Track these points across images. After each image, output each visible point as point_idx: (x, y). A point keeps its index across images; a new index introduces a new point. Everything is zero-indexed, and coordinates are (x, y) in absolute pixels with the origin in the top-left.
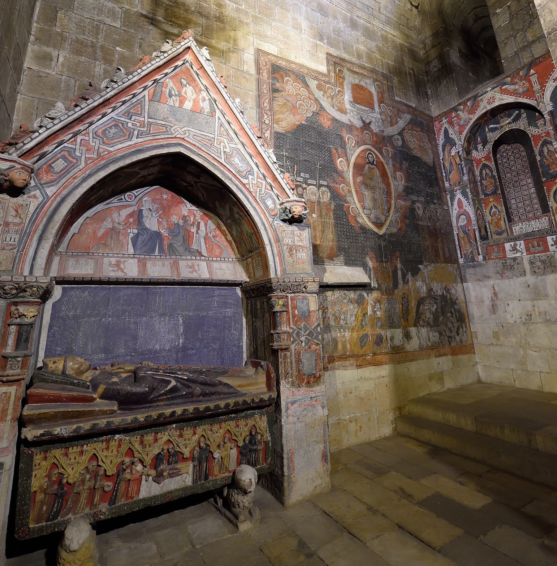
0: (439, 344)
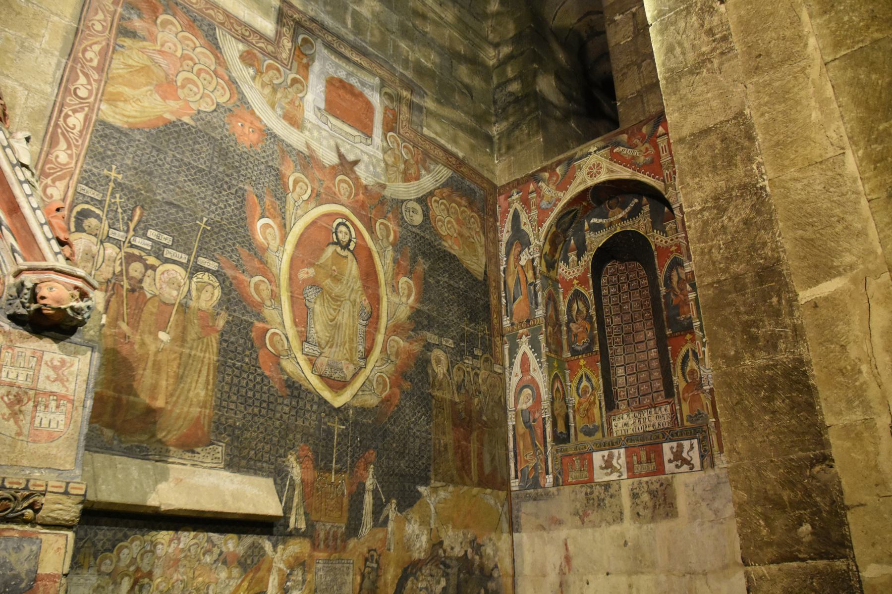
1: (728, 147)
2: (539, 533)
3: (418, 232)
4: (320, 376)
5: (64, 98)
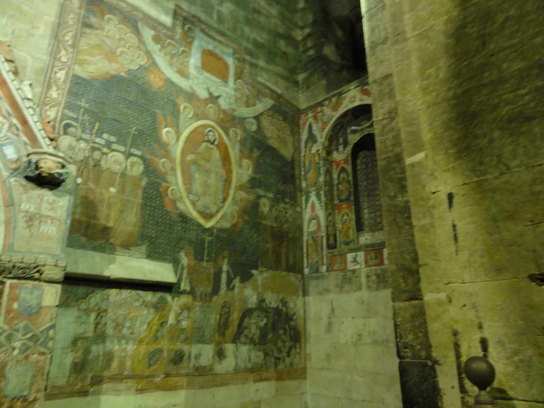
3: (254, 135)
5: (53, 63)
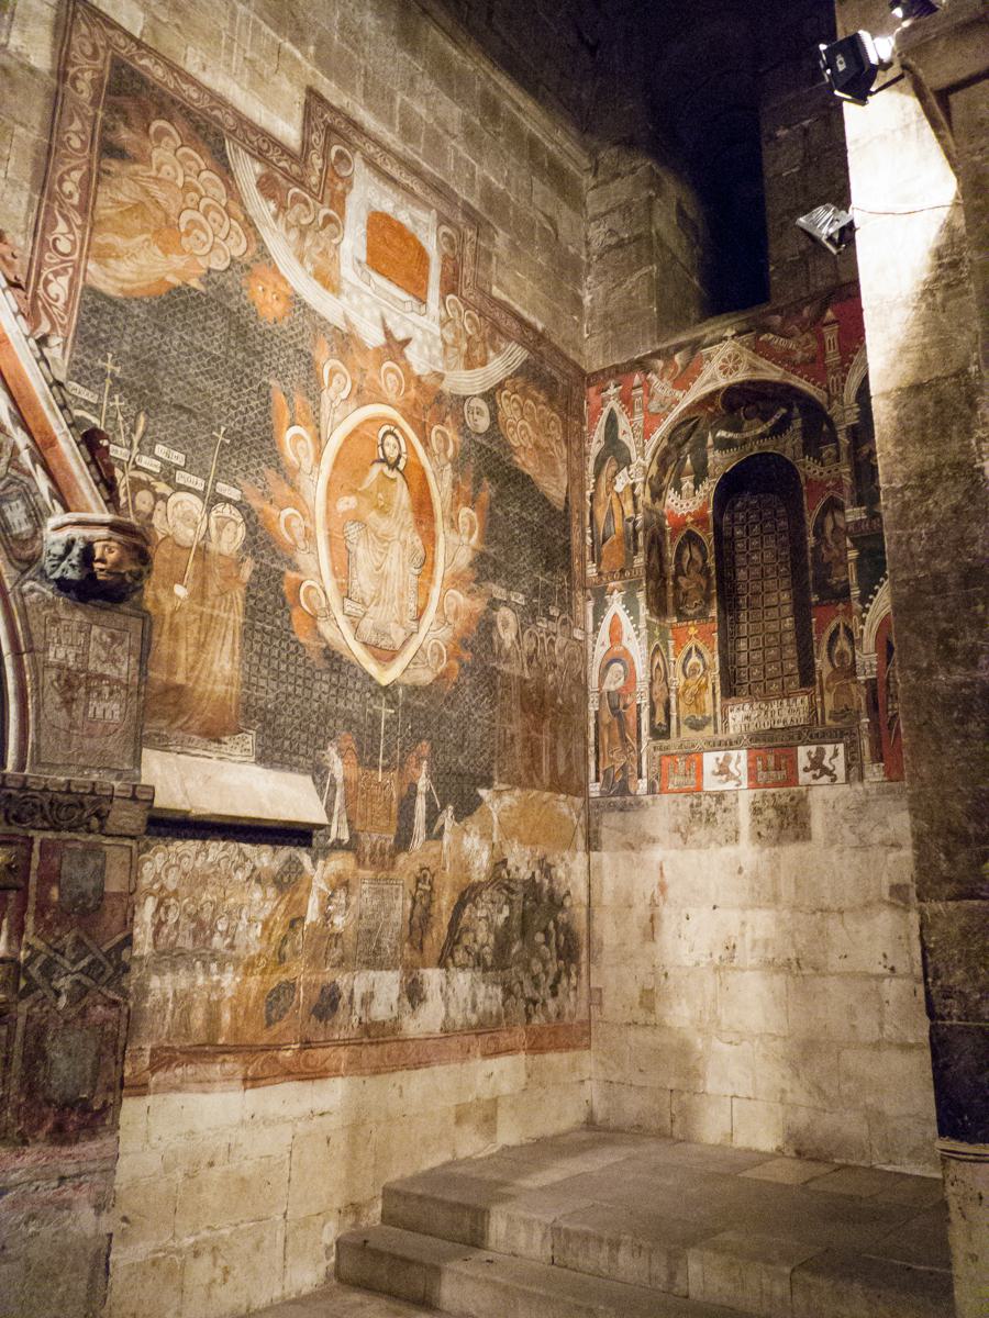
0: (499, 1023)
1: (943, 412)
2: (626, 853)
3: (484, 442)
4: (365, 643)
